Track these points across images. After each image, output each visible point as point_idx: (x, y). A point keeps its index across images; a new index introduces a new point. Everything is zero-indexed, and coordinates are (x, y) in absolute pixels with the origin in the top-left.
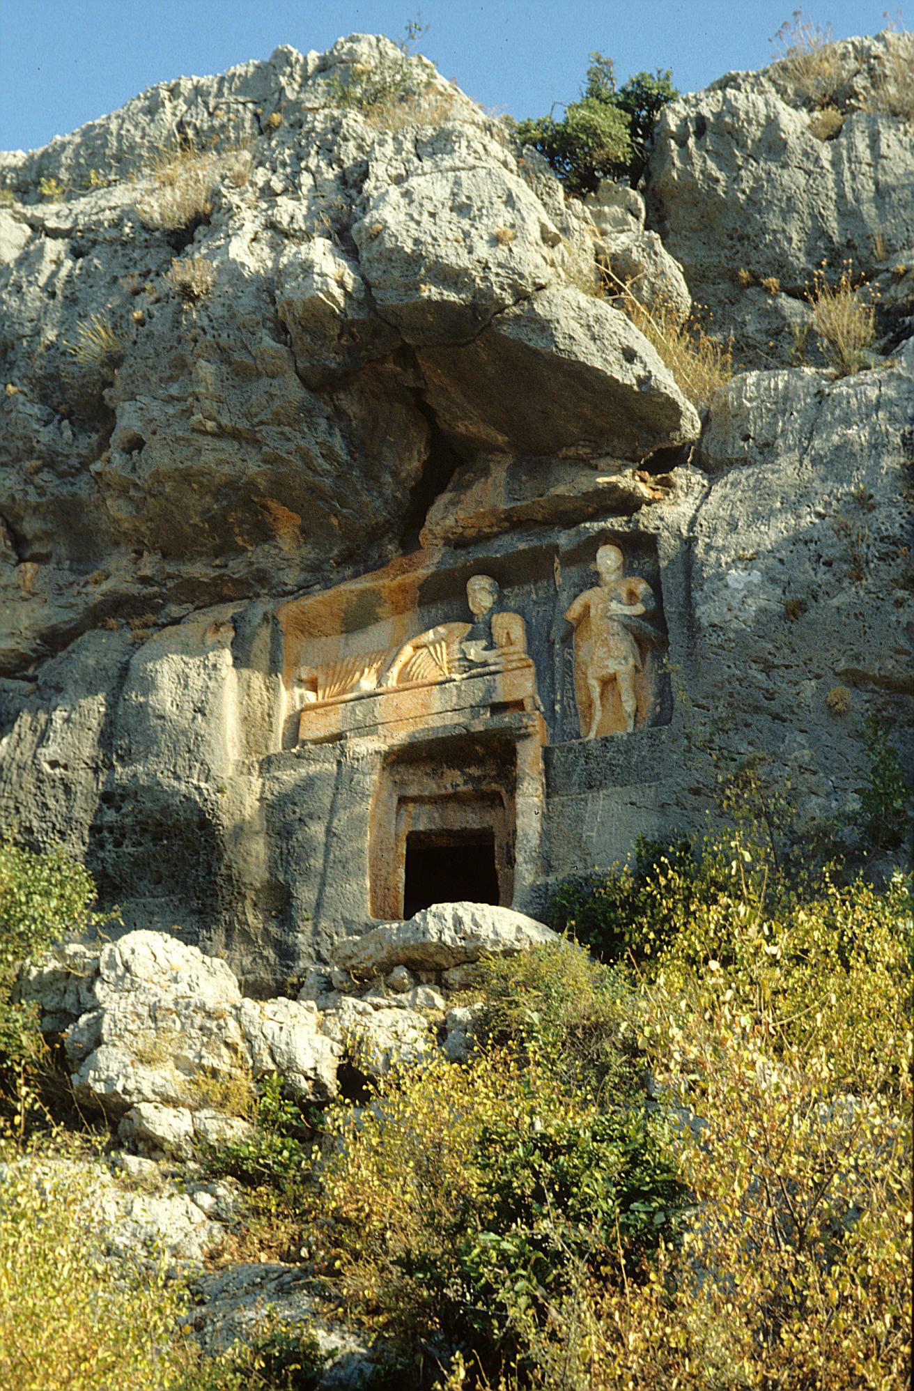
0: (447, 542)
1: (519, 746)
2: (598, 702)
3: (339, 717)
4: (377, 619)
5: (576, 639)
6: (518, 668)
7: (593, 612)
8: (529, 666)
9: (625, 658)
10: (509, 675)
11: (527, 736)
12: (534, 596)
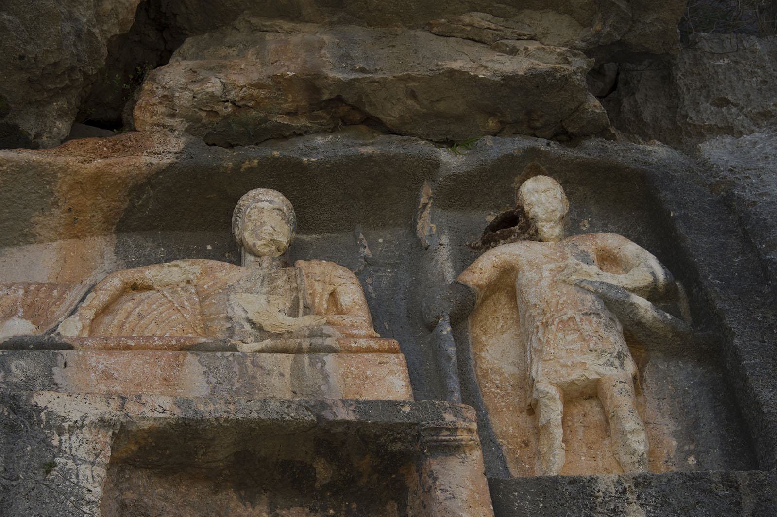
0: (195, 127)
1: (434, 465)
2: (558, 432)
5: (474, 331)
6: (368, 350)
7: (526, 276)
8: (391, 351)
9: (620, 356)
10: (355, 359)
11: (452, 449)
12: (366, 251)
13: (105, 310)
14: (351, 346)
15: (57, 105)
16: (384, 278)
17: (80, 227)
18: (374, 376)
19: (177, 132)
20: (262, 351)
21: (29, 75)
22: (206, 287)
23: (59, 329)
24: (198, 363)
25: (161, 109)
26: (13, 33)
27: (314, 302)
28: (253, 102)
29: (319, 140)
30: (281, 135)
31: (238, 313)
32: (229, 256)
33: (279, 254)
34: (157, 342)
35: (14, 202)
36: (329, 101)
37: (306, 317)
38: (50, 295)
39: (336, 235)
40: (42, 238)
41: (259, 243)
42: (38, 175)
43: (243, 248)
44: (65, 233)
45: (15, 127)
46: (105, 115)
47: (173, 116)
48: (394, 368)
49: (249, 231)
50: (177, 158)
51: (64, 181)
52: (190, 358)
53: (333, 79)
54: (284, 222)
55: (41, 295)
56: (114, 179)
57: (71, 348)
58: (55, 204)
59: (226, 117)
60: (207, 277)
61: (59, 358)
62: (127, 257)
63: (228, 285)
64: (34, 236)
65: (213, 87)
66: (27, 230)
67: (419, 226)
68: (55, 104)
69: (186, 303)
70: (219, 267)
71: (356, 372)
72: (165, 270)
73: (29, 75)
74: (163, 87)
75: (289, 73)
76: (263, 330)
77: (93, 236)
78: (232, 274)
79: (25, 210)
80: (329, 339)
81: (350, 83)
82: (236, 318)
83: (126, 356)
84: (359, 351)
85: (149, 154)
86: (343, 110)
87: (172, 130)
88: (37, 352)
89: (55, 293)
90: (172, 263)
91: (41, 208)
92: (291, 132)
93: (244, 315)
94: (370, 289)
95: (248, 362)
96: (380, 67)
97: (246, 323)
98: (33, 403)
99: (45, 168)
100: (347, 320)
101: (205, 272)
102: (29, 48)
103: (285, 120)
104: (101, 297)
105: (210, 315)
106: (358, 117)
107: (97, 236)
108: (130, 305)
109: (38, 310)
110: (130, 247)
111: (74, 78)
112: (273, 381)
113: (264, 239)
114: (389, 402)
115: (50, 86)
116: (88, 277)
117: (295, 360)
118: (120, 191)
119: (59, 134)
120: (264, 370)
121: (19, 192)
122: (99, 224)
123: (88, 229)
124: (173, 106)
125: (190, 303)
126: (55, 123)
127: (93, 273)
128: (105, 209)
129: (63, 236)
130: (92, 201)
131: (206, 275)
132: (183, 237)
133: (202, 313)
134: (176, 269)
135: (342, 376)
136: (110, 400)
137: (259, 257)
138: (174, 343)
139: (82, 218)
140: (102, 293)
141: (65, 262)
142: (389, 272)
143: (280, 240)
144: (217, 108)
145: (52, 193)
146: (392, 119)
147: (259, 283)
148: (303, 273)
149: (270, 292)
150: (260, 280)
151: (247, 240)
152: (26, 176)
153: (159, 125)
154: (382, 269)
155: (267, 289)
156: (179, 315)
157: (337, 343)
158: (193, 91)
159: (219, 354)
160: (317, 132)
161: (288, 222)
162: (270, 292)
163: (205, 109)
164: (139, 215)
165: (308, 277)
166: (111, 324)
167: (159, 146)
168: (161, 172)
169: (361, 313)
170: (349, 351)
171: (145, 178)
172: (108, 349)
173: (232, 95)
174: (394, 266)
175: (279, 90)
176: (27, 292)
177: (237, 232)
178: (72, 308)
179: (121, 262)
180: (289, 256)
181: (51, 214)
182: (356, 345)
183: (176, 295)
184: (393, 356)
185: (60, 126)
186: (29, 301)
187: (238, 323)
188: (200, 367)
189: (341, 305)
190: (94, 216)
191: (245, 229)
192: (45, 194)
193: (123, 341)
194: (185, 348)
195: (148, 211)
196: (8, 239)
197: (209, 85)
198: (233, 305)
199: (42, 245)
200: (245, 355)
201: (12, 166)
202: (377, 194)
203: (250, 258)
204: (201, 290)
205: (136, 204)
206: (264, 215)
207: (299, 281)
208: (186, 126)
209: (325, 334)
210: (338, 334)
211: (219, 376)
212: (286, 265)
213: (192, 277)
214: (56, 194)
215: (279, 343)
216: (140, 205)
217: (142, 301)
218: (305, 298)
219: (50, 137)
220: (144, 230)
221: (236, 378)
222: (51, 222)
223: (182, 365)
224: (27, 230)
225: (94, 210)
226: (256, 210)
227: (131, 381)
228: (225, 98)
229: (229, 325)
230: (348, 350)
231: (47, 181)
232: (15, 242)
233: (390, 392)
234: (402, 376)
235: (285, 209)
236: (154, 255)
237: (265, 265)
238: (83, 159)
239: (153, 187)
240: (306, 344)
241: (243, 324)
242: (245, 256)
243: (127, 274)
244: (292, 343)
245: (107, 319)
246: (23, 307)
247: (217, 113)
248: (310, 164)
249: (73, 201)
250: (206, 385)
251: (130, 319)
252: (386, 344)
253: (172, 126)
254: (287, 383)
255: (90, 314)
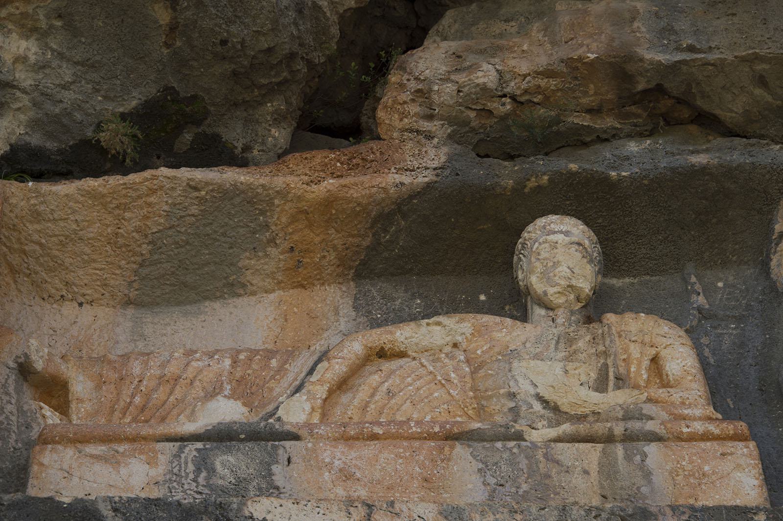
3: (159, 471)
4: (234, 288)
6: (706, 437)
8: (736, 437)
10: (687, 451)
12: (701, 300)
13: (342, 385)
14: (682, 432)
15: (272, 106)
16: (726, 337)
17: (305, 272)
18: (714, 473)
19: (436, 140)
20: (558, 440)
21: (233, 66)
22: (479, 352)
23: (280, 413)
24: (470, 457)
25: (414, 109)
26: (212, 9)
27: (629, 371)
28: (540, 97)
29: (633, 147)
30: (579, 140)
31: (524, 388)
32: (510, 310)
33: (580, 305)
34: (414, 429)
35: (216, 240)
36: (645, 92)
37: (618, 392)
38: (267, 366)
39: (658, 277)
40: (254, 288)
41: (551, 290)
42: (248, 203)
43: (529, 298)
44: (285, 280)
45: (216, 138)
46: (337, 119)
47: (430, 117)
48: (742, 461)
49: (538, 275)
50: (437, 175)
51: (283, 210)
52: (460, 450)
53: (651, 62)
54: (585, 260)
55: (255, 366)
56: (351, 205)
57: (296, 437)
58: (272, 241)
59: (503, 118)
60: (480, 339)
61: (281, 451)
62: (370, 312)
63: (510, 349)
64: (244, 286)
65: (485, 76)
66: (235, 277)
67: (773, 263)
68: (269, 105)
69: (453, 375)
70: (496, 324)
71: (690, 467)
72: (424, 330)
73: (233, 66)
74: (417, 79)
75: (589, 55)
76: (560, 411)
77: (323, 284)
78: (515, 334)
79: (231, 251)
80: (650, 422)
81: (675, 67)
82: (522, 395)
83: (373, 447)
84: (692, 438)
85: (398, 171)
86: (665, 104)
87: (429, 137)
88: (250, 444)
89: (274, 363)
90: (433, 319)
91: (252, 247)
92: (594, 137)
93: (532, 391)
94: (707, 352)
95: (540, 455)
96: (715, 43)
97: (535, 401)
98: (247, 514)
99: (258, 193)
100: (676, 396)
101: (478, 332)
102: (234, 29)
103: (585, 121)
104: (336, 368)
105: (486, 391)
106: (686, 113)
107: (328, 285)
108: (375, 378)
109: (251, 387)
110: (374, 298)
111: (295, 69)
112: (574, 481)
113: (557, 284)
114: (736, 507)
115: (264, 81)
116: (318, 341)
117: (604, 451)
118: (360, 222)
119: (275, 146)
120: (562, 466)
121: (223, 226)
122: (332, 268)
123: (316, 275)
124: (431, 104)
125: (458, 375)
126: (270, 130)
127: (325, 335)
128: (340, 247)
129: (283, 285)
130: (322, 236)
131: (480, 337)
132: (447, 283)
133: (474, 389)
134: (438, 328)
135: (671, 473)
136: (352, 509)
137: (552, 309)
138: (437, 429)
139: (308, 260)
140: (337, 363)
141: (286, 320)
142: (733, 329)
143: (581, 285)
144: (490, 105)
145: (267, 226)
146: (734, 115)
147: (553, 346)
148: (614, 332)
149: (569, 358)
150: (554, 342)
151: (534, 286)
152: (232, 204)
153: (411, 131)
154: (723, 324)
155: (564, 354)
156: (442, 391)
157: (662, 427)
158: (457, 82)
159: (499, 445)
160: (630, 136)
161: (591, 261)
162: (569, 358)
163: (474, 107)
164: (386, 254)
165: (620, 336)
166: (350, 405)
167: (412, 160)
168: (416, 196)
169: (695, 385)
170: (679, 438)
171: (393, 203)
172: (347, 439)
173: (512, 87)
174: (739, 319)
175: (576, 78)
176: (235, 362)
177: (520, 276)
178: (297, 383)
179: (363, 319)
180: (595, 308)
181: (267, 256)
182: (689, 430)
183: (439, 364)
184: (741, 444)
185: (277, 134)
186: (238, 375)
187: (525, 401)
188: (474, 462)
189: (667, 375)
190: (324, 257)
191: (532, 272)
192: (258, 228)
193: (367, 428)
194: (452, 437)
195: (398, 249)
196: (208, 290)
197: (480, 74)
198: (517, 377)
199: (254, 298)
200: (534, 446)
201: (212, 191)
202: (714, 220)
203: (539, 312)
204: (473, 356)
205: (383, 240)
206: (558, 251)
207: (607, 343)
208: (449, 131)
209: (645, 415)
210: (664, 415)
211: (500, 475)
212: (589, 320)
213: (459, 339)
214: (273, 228)
215: (583, 428)
216: (387, 241)
217: (392, 372)
218: (616, 366)
219: (263, 151)
220: (393, 275)
221: (523, 478)
222: (266, 267)
223: (449, 460)
224: (235, 277)
225: (324, 249)
226: (547, 245)
227: (379, 482)
228: (501, 91)
229: (512, 404)
230: (678, 438)
231: (260, 210)
232: (218, 294)
233: (736, 495)
234: (753, 472)
235: (587, 243)
236: (407, 309)
237: (560, 320)
238: (309, 180)
239: (404, 216)
240: (619, 429)
241: (532, 403)
242: (532, 309)
243: (371, 335)
244: (600, 428)
245: (345, 399)
246: (230, 382)
247: (490, 112)
248: (621, 180)
249: (296, 237)
250: (483, 487)
251: (377, 398)
252: (729, 428)
253: (429, 131)
254: (594, 483)
255: (321, 392)
